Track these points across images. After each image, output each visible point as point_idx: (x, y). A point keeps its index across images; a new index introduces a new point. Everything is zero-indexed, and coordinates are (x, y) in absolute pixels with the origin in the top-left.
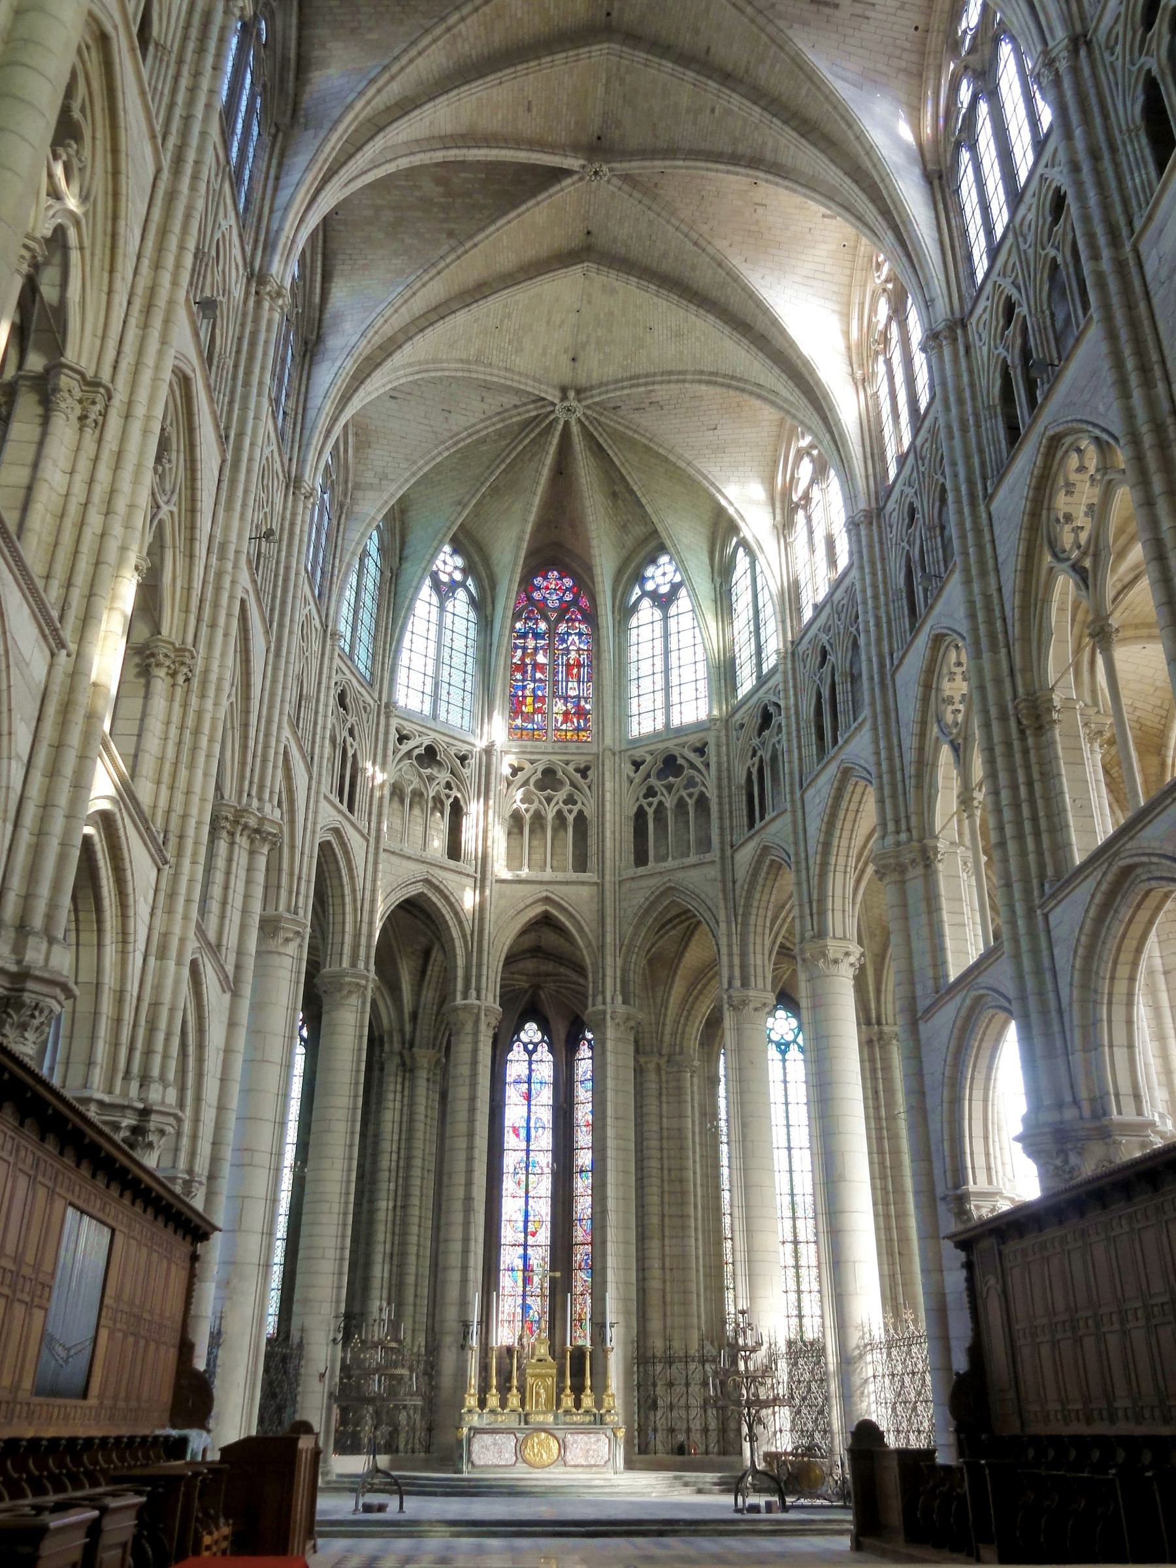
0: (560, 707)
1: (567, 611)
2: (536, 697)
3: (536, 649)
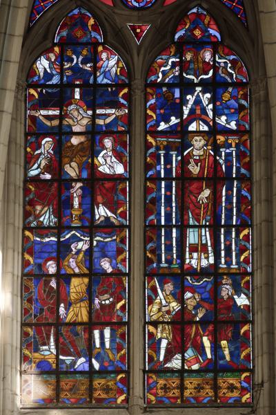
0: (165, 302)
2: (94, 276)
3: (94, 134)
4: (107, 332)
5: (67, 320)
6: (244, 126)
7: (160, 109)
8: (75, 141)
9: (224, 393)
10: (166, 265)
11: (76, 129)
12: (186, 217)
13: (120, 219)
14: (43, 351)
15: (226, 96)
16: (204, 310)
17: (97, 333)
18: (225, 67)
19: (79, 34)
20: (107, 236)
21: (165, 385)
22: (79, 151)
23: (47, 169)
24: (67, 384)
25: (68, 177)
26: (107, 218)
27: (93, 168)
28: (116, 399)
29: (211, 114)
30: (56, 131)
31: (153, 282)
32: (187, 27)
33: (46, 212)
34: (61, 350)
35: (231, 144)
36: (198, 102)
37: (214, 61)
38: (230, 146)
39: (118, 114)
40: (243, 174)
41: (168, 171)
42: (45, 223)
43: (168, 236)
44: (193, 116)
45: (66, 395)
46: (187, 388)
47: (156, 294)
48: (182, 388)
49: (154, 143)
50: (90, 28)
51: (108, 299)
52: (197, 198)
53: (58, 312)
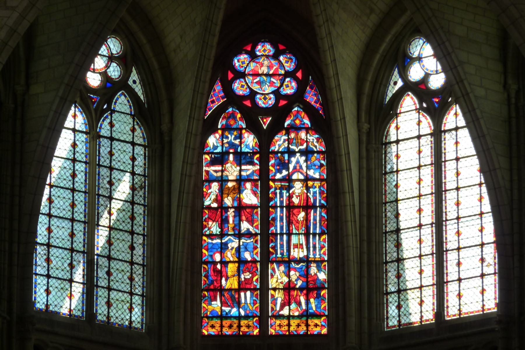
1: (286, 112)
3: (240, 181)
4: (248, 293)
5: (226, 288)
6: (323, 176)
7: (277, 166)
8: (230, 185)
9: (312, 328)
10: (281, 256)
11: (231, 178)
12: (291, 228)
13: (255, 229)
14: (213, 304)
15: (313, 158)
16: (301, 282)
17: (242, 294)
18: (313, 142)
19: (232, 122)
20: (248, 239)
21: (280, 324)
22: (233, 190)
23: (216, 200)
24: (226, 323)
25: (226, 206)
26: (248, 229)
27: (240, 200)
28: (253, 331)
29: (305, 169)
30: (220, 179)
31: (273, 265)
32: (292, 118)
33: (214, 226)
34: (223, 303)
35: (316, 186)
36: (298, 162)
37: (307, 138)
38: (316, 187)
39: (254, 169)
40: (323, 204)
41: (281, 202)
42: (214, 232)
43: (282, 239)
44: (295, 170)
45: (226, 329)
46: (224, 326)
47: (275, 273)
48: (289, 325)
49: (274, 186)
50: (238, 119)
51: (249, 275)
52: (297, 217)
53: (221, 283)
